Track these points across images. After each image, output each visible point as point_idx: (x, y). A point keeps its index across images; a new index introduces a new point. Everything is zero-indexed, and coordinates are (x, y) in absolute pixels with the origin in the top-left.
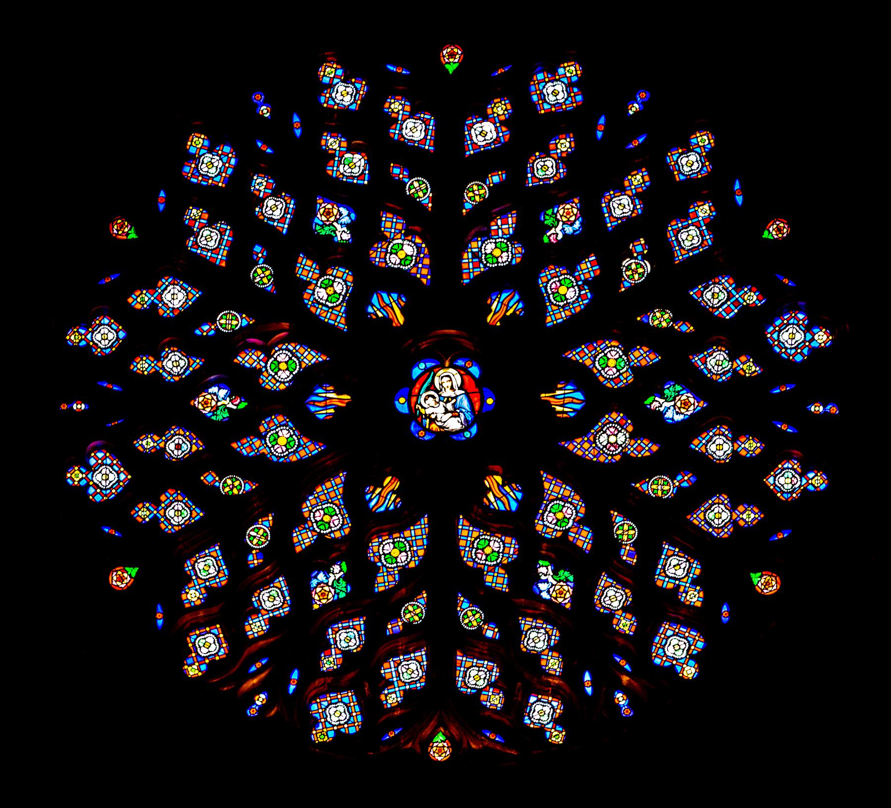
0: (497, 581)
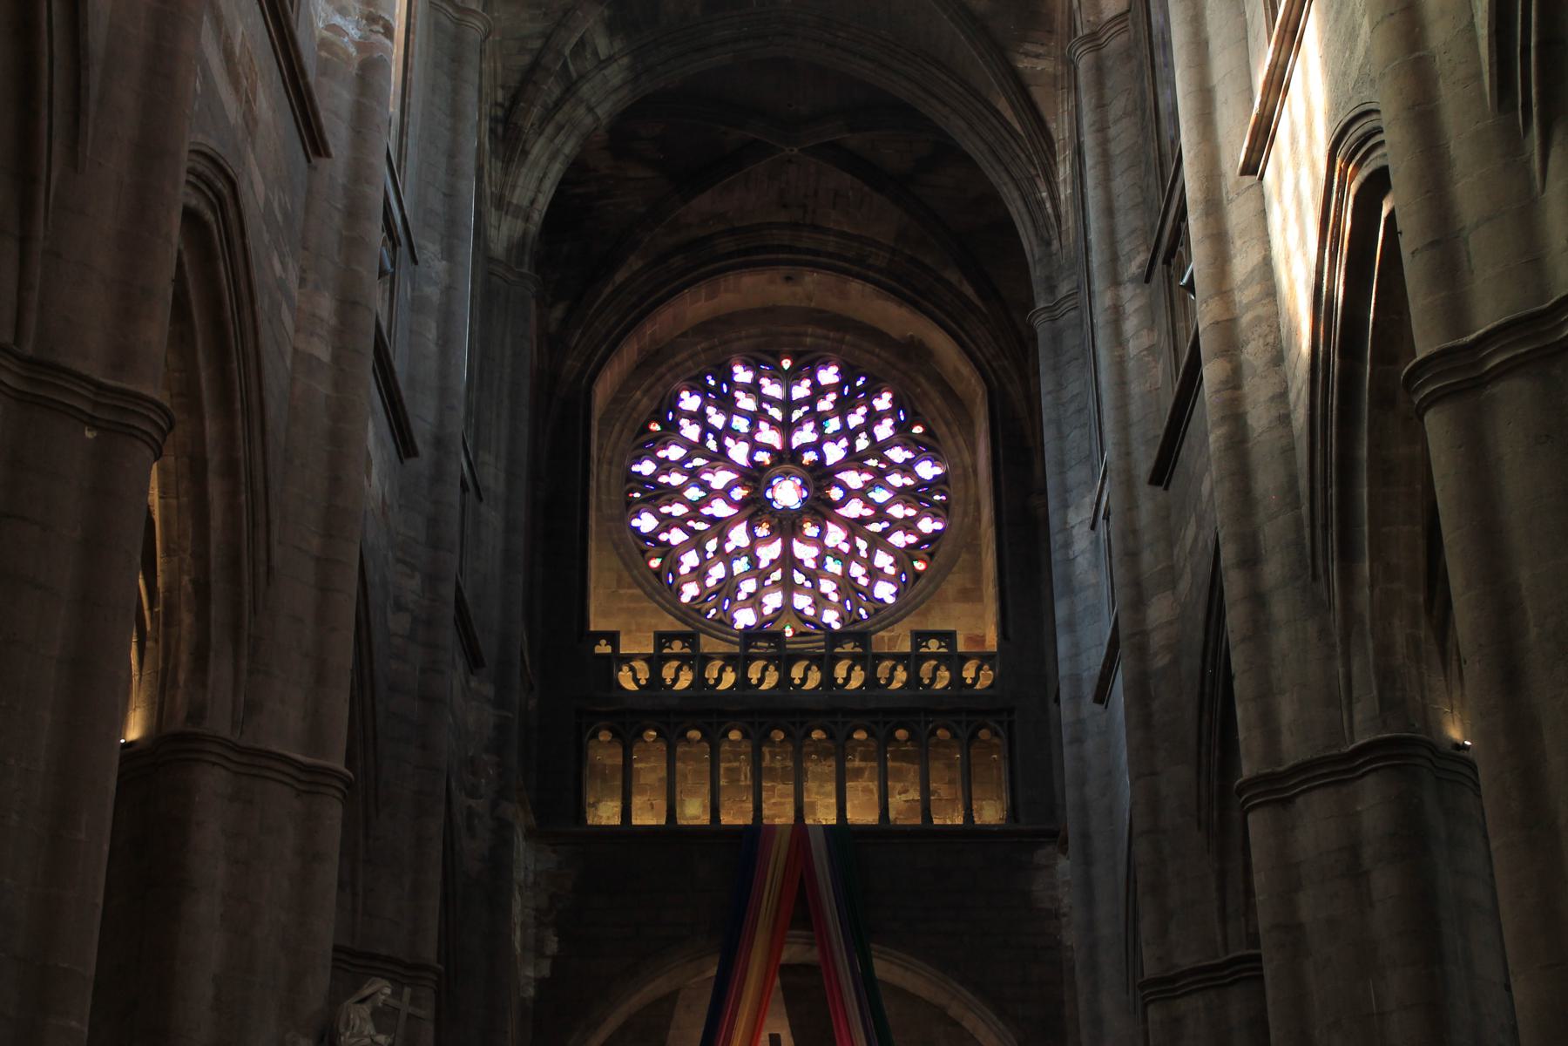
0: (810, 564)
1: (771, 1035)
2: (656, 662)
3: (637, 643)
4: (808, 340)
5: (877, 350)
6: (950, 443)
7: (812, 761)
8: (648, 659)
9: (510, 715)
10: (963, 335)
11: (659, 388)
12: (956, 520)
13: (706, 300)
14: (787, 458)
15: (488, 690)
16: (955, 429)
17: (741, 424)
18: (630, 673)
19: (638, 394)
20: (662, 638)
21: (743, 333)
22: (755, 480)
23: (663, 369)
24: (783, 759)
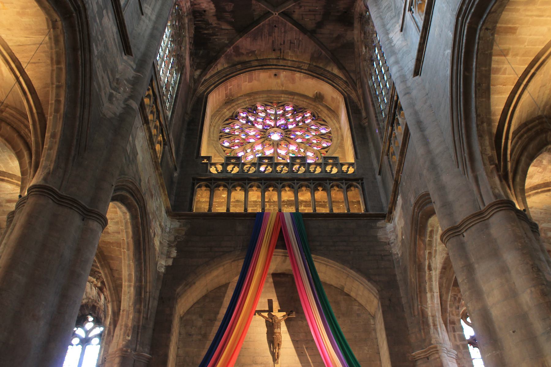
1: (268, 300)
2: (225, 165)
3: (218, 159)
4: (282, 99)
5: (305, 100)
6: (331, 122)
7: (285, 207)
8: (222, 164)
9: (142, 76)
10: (334, 84)
11: (232, 110)
12: (335, 140)
13: (248, 82)
14: (276, 145)
15: (134, 67)
16: (333, 118)
17: (260, 120)
18: (215, 169)
19: (225, 110)
20: (228, 159)
21: (261, 96)
22: (264, 132)
23: (234, 104)
24: (274, 207)
